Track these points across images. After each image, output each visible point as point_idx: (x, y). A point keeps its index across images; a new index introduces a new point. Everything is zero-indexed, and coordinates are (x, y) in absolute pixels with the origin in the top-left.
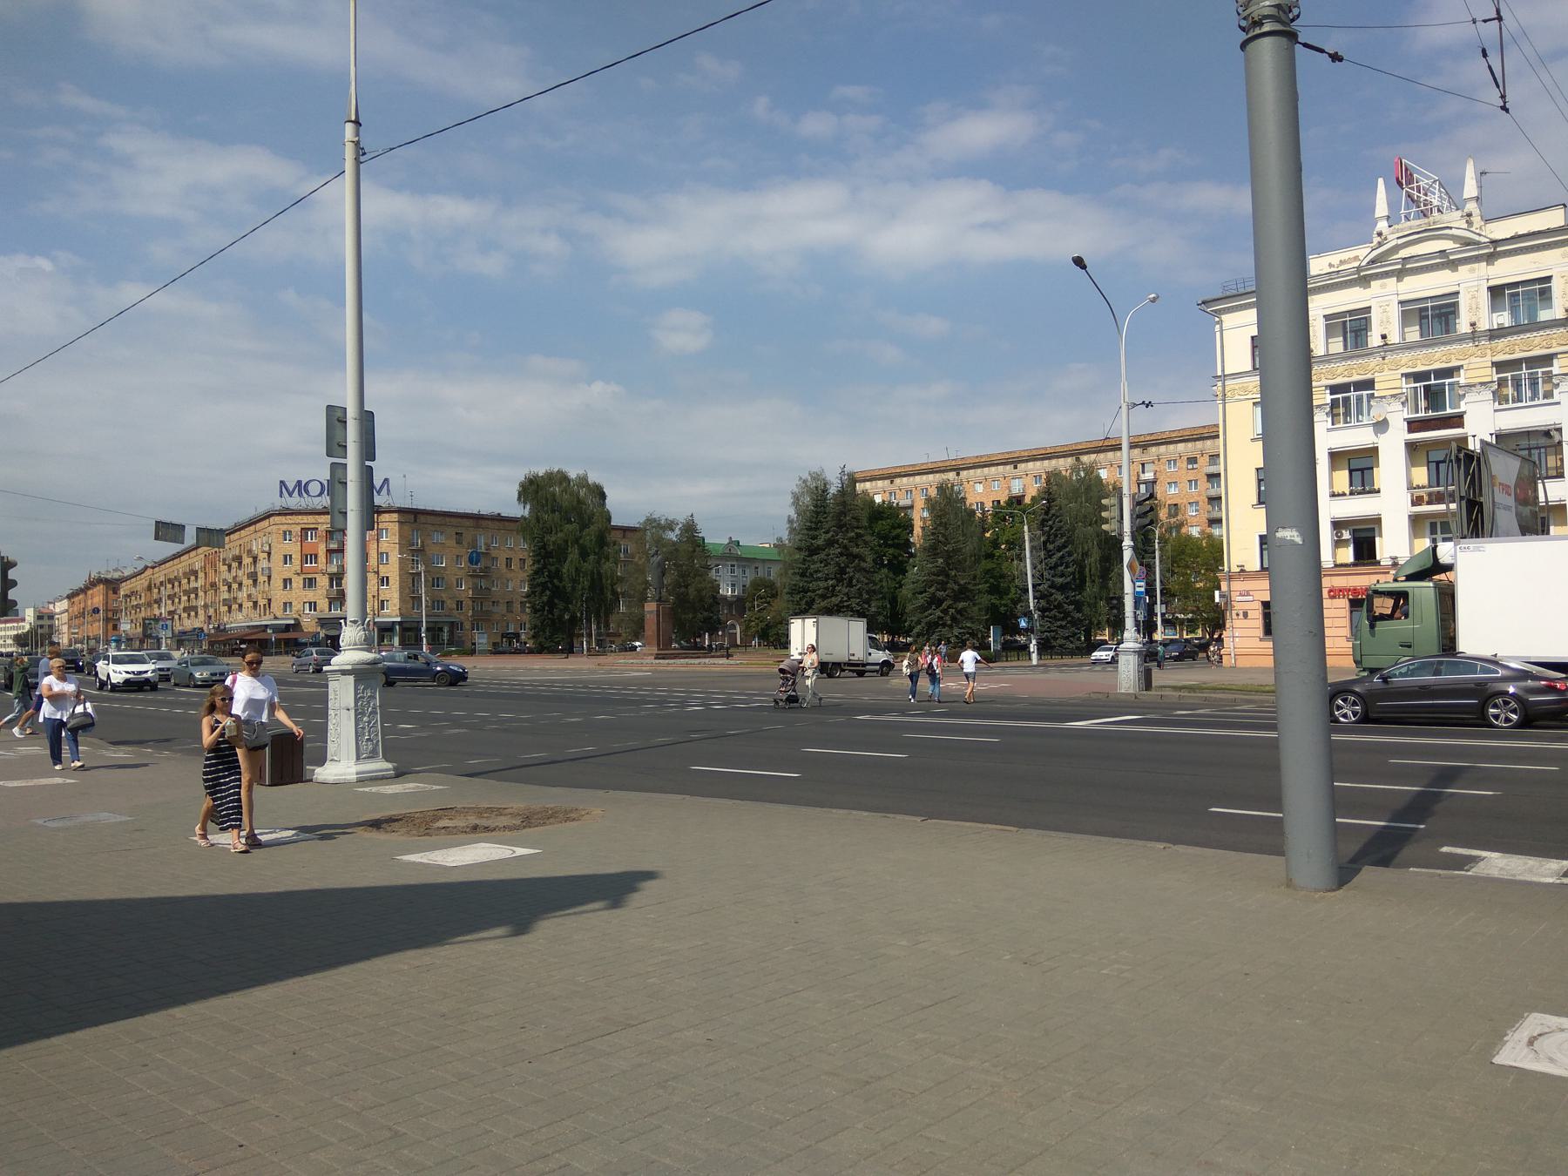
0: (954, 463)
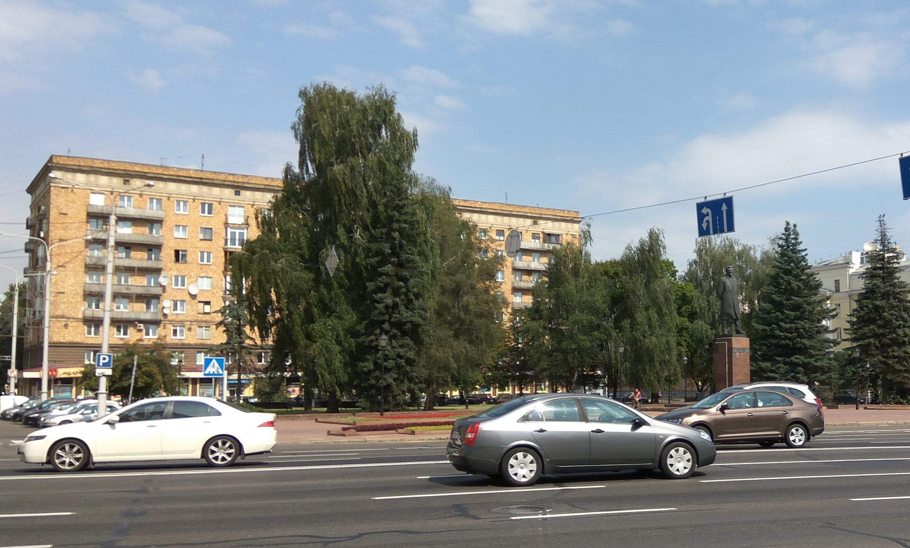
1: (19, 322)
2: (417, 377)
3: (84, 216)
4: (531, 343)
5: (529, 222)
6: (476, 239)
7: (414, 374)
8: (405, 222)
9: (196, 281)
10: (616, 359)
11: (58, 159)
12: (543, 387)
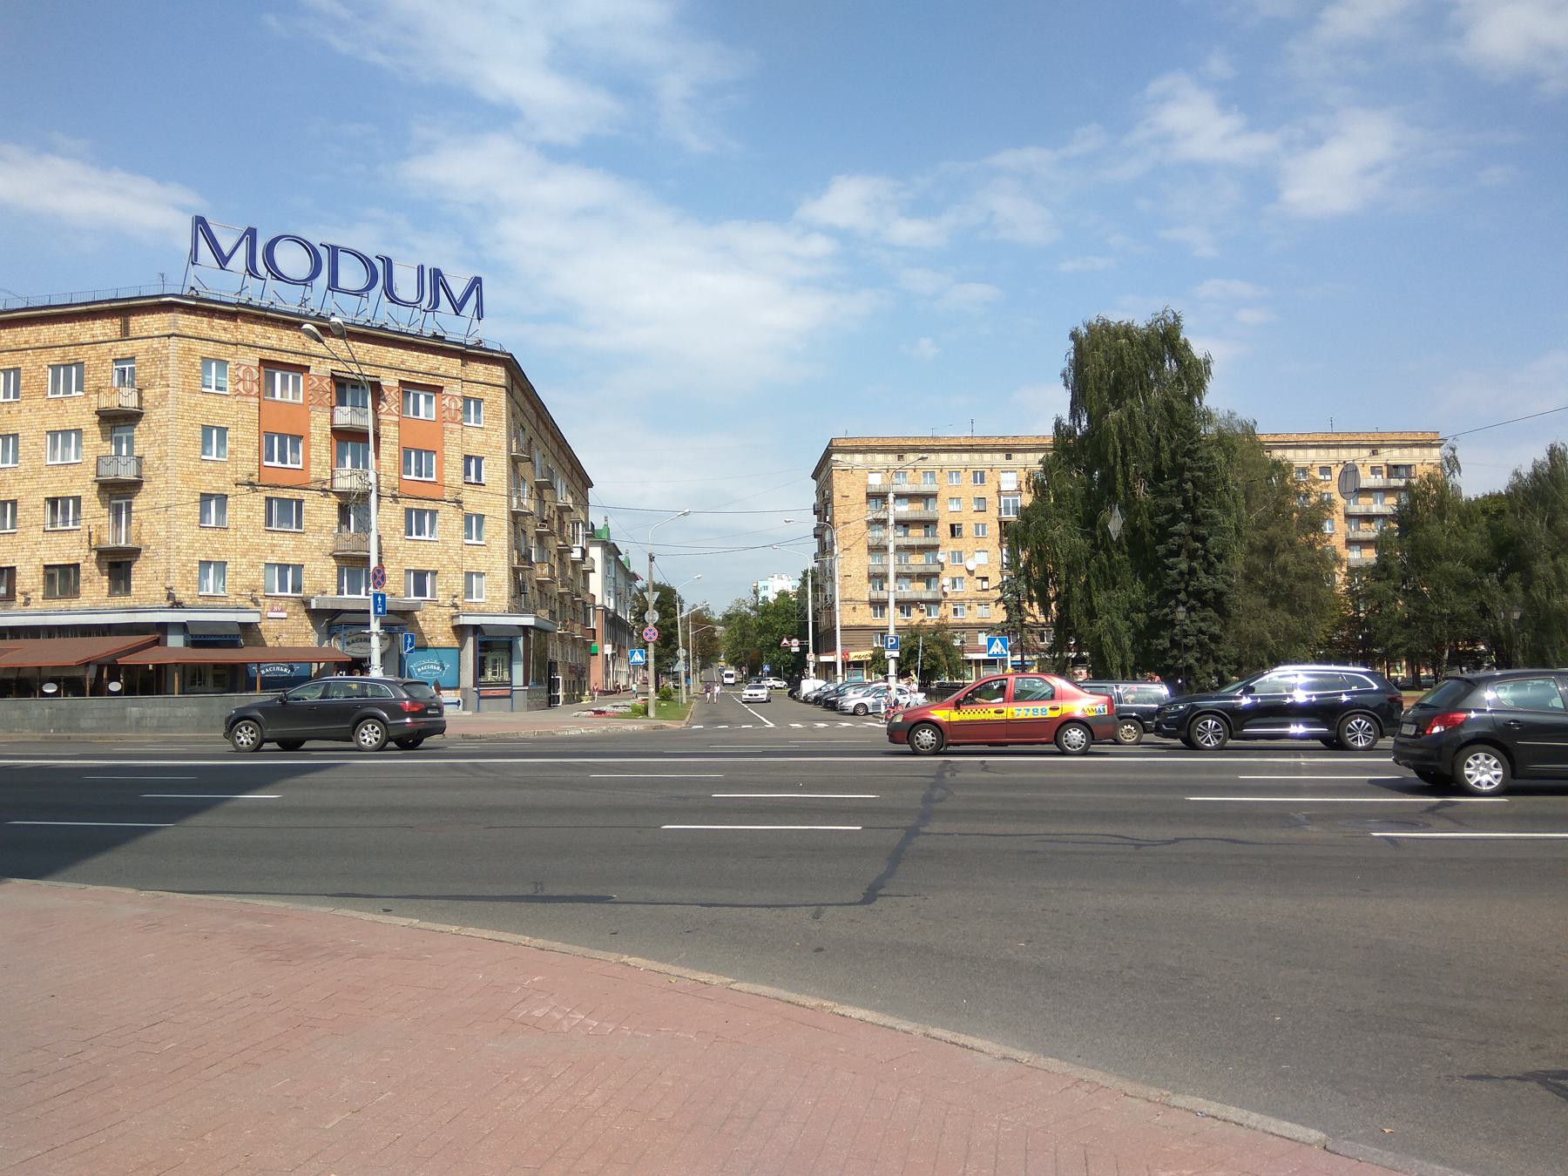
0: (1001, 441)
1: (813, 606)
2: (1225, 657)
3: (864, 497)
4: (1377, 611)
5: (1366, 452)
6: (1293, 481)
7: (1221, 653)
8: (1200, 469)
9: (973, 556)
10: (1507, 628)
11: (838, 441)
12: (1398, 668)
